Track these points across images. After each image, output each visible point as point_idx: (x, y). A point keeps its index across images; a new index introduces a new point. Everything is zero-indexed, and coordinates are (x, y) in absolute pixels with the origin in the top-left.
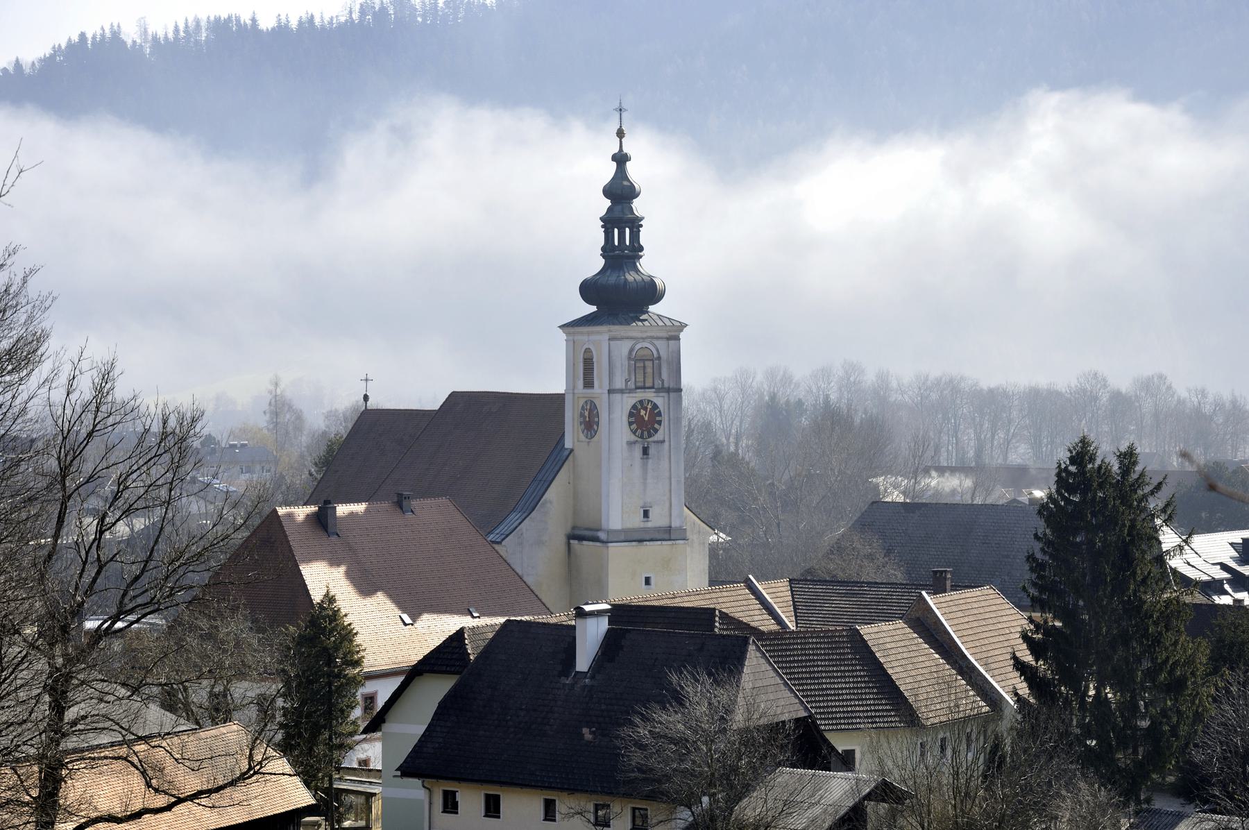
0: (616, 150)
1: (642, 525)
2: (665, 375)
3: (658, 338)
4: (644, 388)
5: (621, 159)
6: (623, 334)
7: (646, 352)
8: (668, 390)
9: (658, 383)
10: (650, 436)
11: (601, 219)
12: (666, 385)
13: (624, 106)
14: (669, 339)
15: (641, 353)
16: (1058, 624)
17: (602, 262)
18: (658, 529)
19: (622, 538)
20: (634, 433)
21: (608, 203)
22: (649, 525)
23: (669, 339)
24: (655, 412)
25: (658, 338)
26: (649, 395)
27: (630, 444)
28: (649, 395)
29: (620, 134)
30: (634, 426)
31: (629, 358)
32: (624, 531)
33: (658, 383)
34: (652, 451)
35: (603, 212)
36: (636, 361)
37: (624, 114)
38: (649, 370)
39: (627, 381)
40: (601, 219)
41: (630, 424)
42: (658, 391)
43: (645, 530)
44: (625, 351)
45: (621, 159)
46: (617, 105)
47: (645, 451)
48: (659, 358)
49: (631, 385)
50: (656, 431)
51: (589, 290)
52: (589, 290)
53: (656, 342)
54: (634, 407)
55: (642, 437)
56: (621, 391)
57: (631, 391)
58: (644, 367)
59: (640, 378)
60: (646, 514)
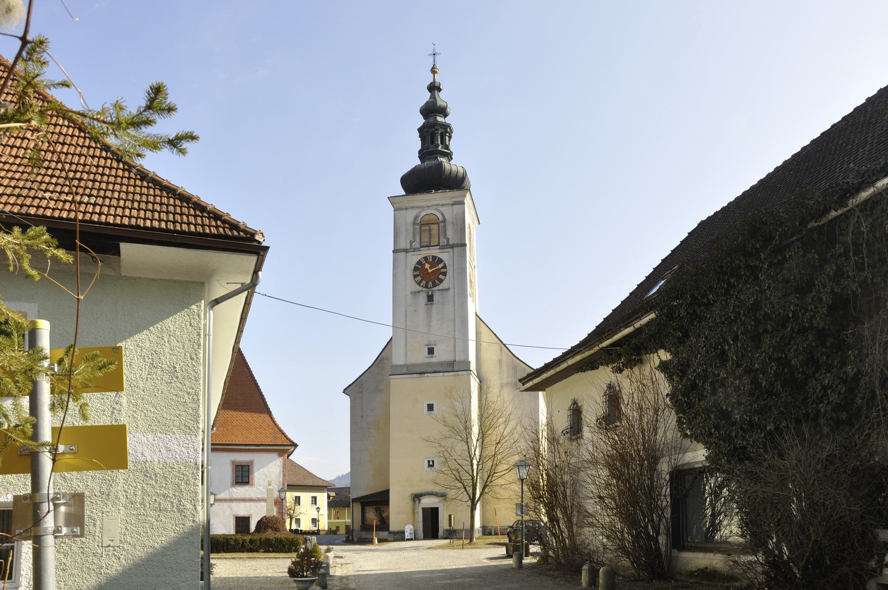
1: (426, 360)
2: (450, 234)
3: (443, 205)
5: (434, 88)
9: (443, 241)
10: (435, 285)
12: (451, 242)
13: (437, 51)
15: (427, 218)
18: (442, 364)
19: (404, 371)
20: (419, 283)
22: (434, 360)
25: (443, 205)
27: (415, 293)
28: (434, 252)
30: (419, 278)
31: (414, 224)
33: (443, 241)
36: (421, 225)
37: (437, 57)
38: (435, 232)
39: (411, 243)
41: (415, 276)
42: (442, 248)
43: (429, 364)
45: (434, 88)
46: (431, 52)
47: (430, 298)
48: (444, 221)
49: (416, 245)
50: (441, 281)
53: (441, 209)
54: (419, 263)
55: (426, 286)
56: (406, 251)
57: (415, 250)
58: (430, 230)
59: (425, 239)
60: (431, 351)
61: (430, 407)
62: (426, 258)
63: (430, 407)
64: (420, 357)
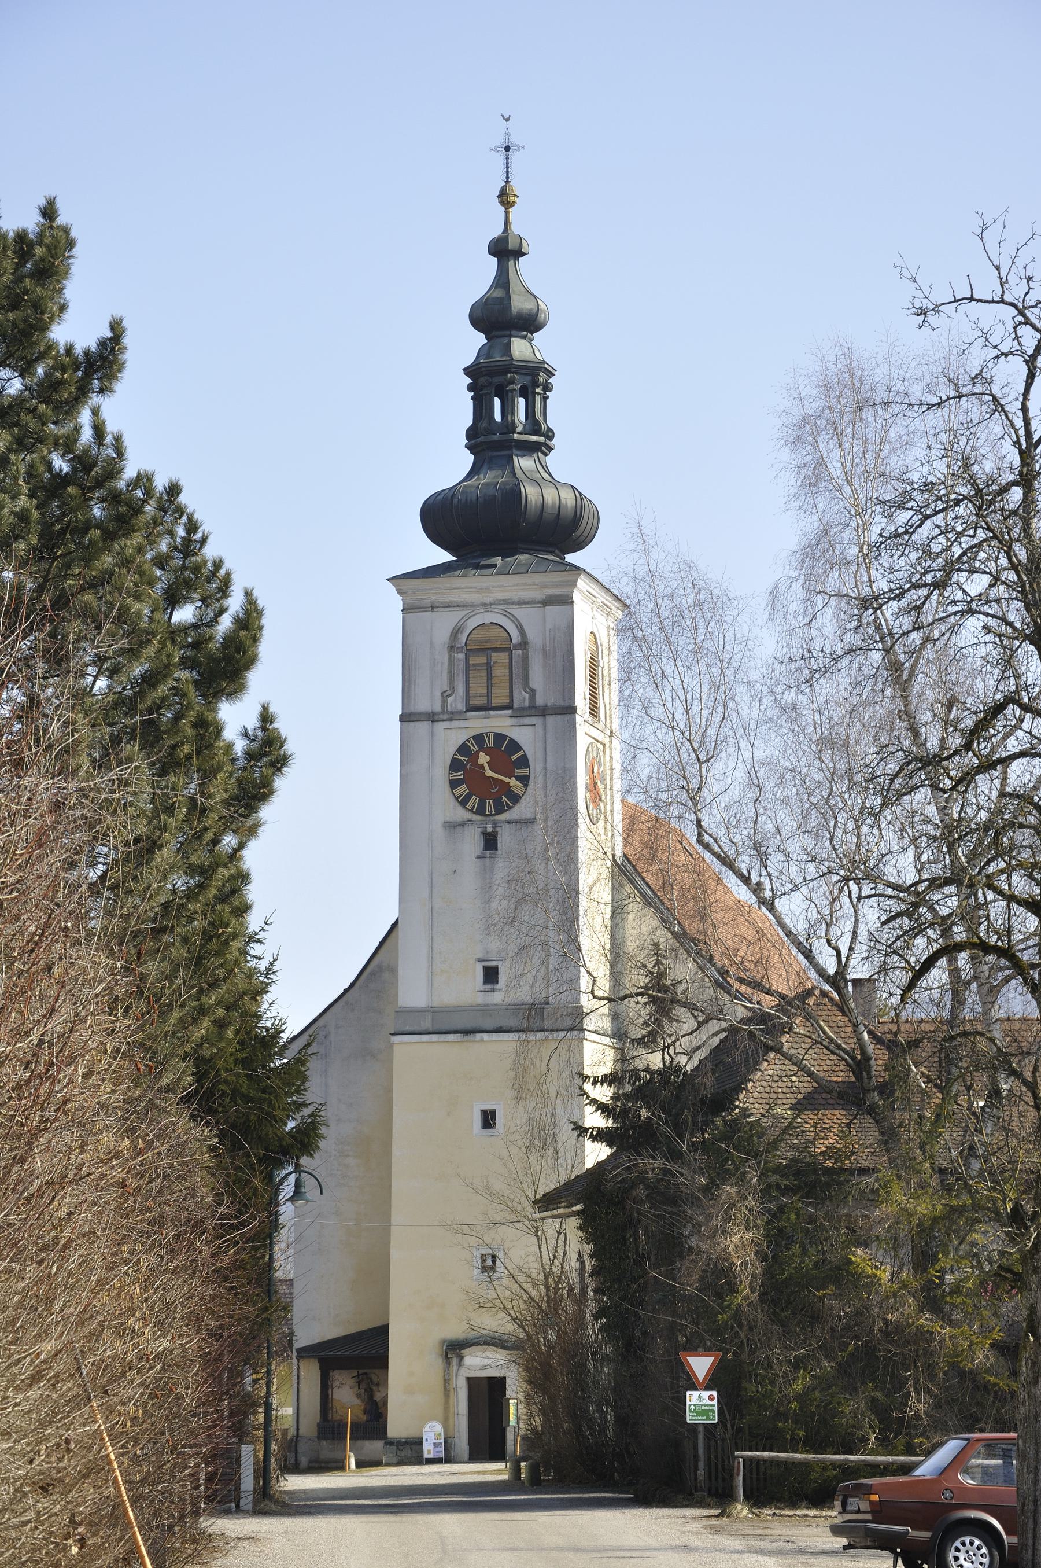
0: (498, 231)
1: (480, 999)
2: (537, 678)
3: (521, 603)
4: (487, 708)
5: (505, 250)
6: (435, 598)
7: (494, 633)
8: (543, 712)
9: (521, 698)
10: (500, 809)
11: (468, 371)
12: (540, 701)
13: (515, 139)
14: (547, 602)
15: (482, 635)
16: (291, 1124)
17: (471, 458)
18: (514, 1009)
19: (427, 1024)
20: (463, 803)
21: (481, 339)
22: (497, 998)
23: (547, 602)
24: (508, 754)
25: (521, 603)
26: (499, 723)
27: (452, 827)
28: (499, 723)
29: (506, 199)
30: (463, 789)
31: (452, 648)
32: (433, 1011)
33: (521, 698)
34: (505, 840)
35: (470, 359)
36: (470, 651)
37: (515, 157)
38: (500, 672)
39: (445, 696)
40: (468, 371)
41: (454, 784)
42: (520, 713)
43: (485, 1009)
44: (442, 634)
45: (505, 250)
46: (499, 140)
47: (490, 842)
48: (524, 644)
49: (457, 703)
50: (516, 799)
51: (441, 517)
52: (441, 517)
53: (516, 612)
54: (463, 749)
55: (481, 811)
56: (431, 717)
57: (453, 716)
58: (489, 667)
59: (479, 689)
60: (491, 975)
61: (488, 1119)
62: (479, 739)
63: (488, 1119)
64: (465, 989)
